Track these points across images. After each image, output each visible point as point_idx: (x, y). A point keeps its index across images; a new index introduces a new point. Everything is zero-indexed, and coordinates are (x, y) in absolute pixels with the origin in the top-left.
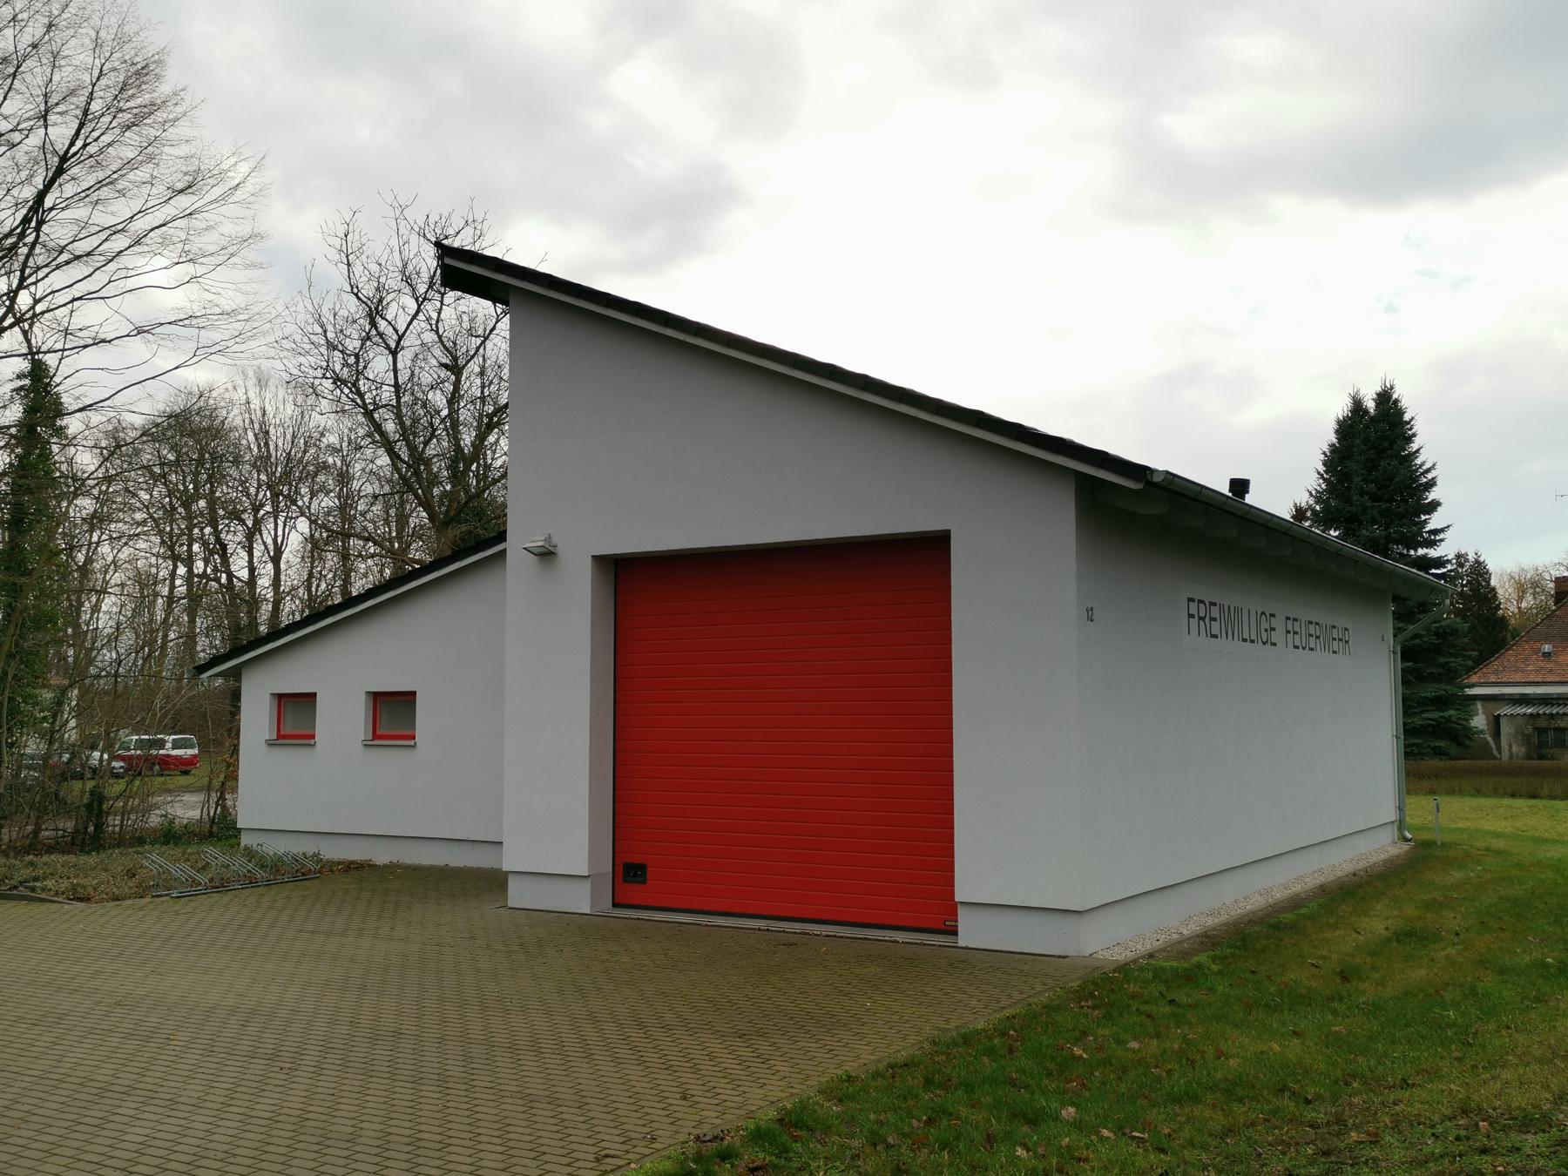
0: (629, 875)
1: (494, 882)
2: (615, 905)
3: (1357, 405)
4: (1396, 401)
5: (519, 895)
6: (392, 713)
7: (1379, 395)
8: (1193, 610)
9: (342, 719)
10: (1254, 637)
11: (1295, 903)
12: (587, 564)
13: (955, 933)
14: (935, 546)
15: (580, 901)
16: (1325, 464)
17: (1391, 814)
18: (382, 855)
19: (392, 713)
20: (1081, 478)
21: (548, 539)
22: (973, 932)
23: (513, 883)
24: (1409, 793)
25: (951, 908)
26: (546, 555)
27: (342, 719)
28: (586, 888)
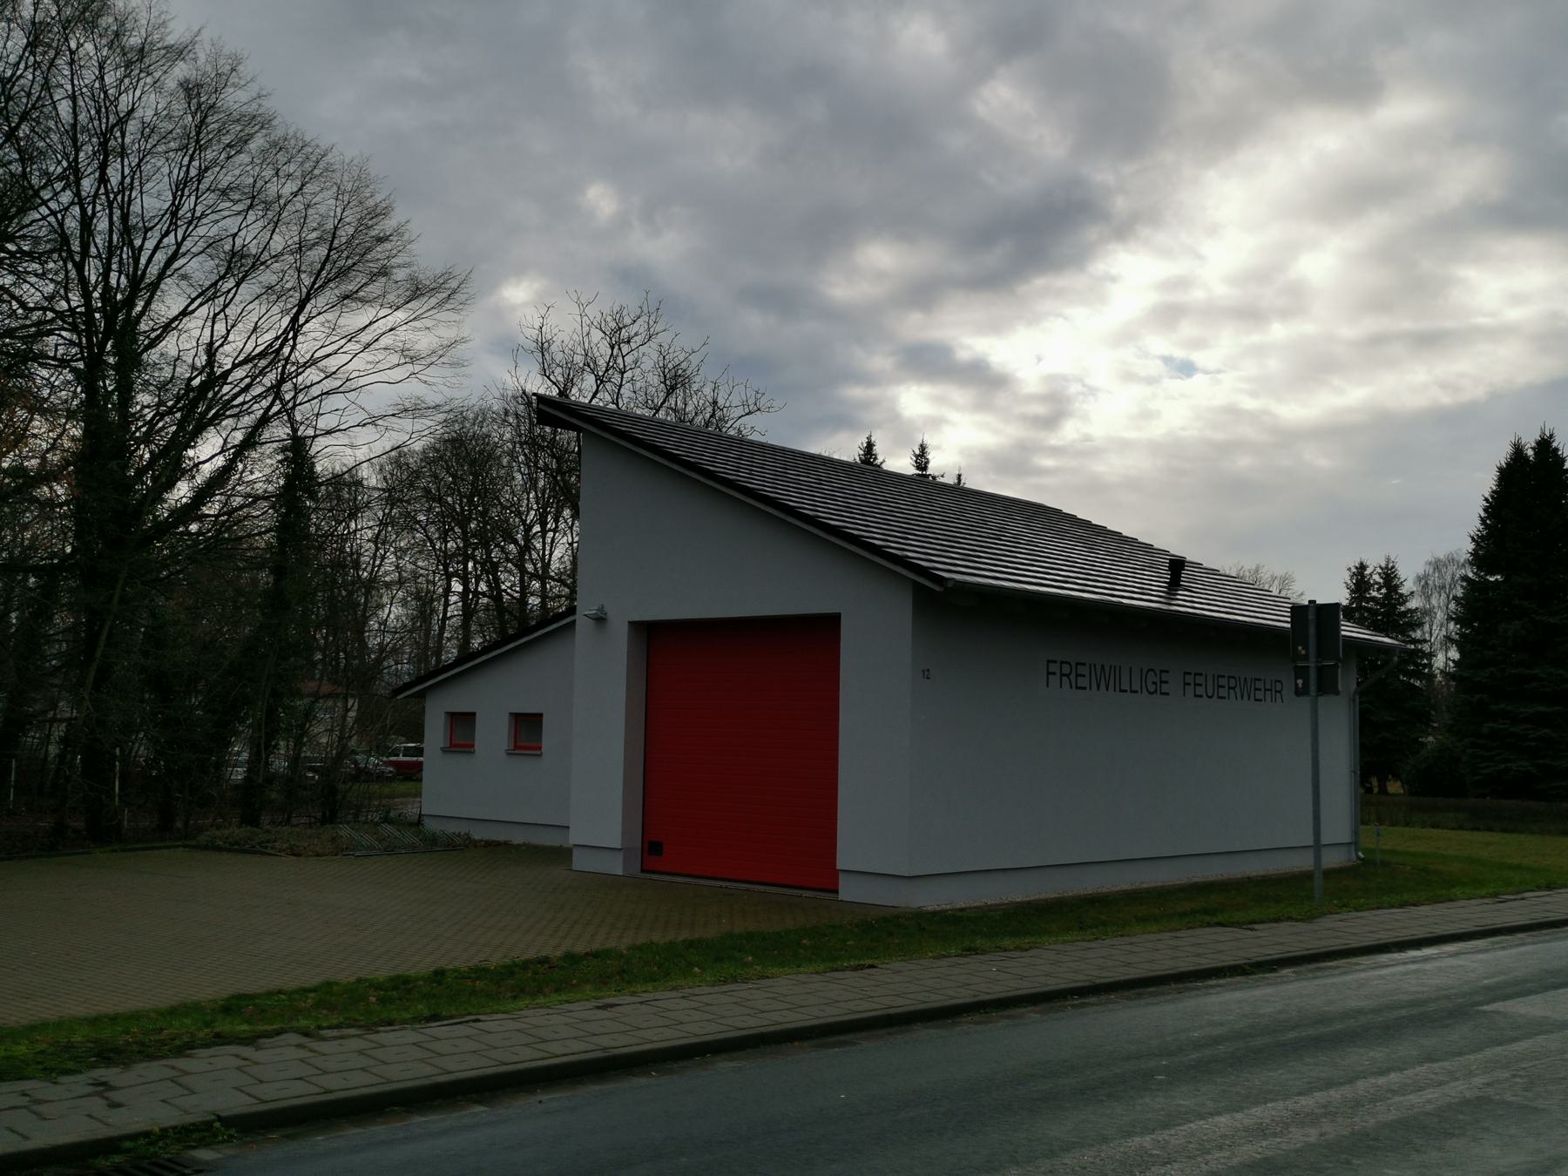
0: (653, 850)
1: (562, 855)
2: (643, 871)
3: (1518, 451)
4: (1556, 449)
5: (581, 862)
6: (527, 728)
7: (1538, 443)
8: (1053, 668)
9: (492, 734)
10: (1136, 687)
11: (1148, 891)
12: (625, 628)
13: (836, 892)
14: (828, 625)
15: (616, 866)
16: (1485, 510)
17: (1347, 838)
18: (518, 837)
19: (527, 728)
20: (915, 583)
21: (601, 609)
22: (848, 891)
23: (576, 853)
24: (1364, 822)
25: (835, 874)
26: (600, 619)
27: (492, 734)
28: (620, 857)
